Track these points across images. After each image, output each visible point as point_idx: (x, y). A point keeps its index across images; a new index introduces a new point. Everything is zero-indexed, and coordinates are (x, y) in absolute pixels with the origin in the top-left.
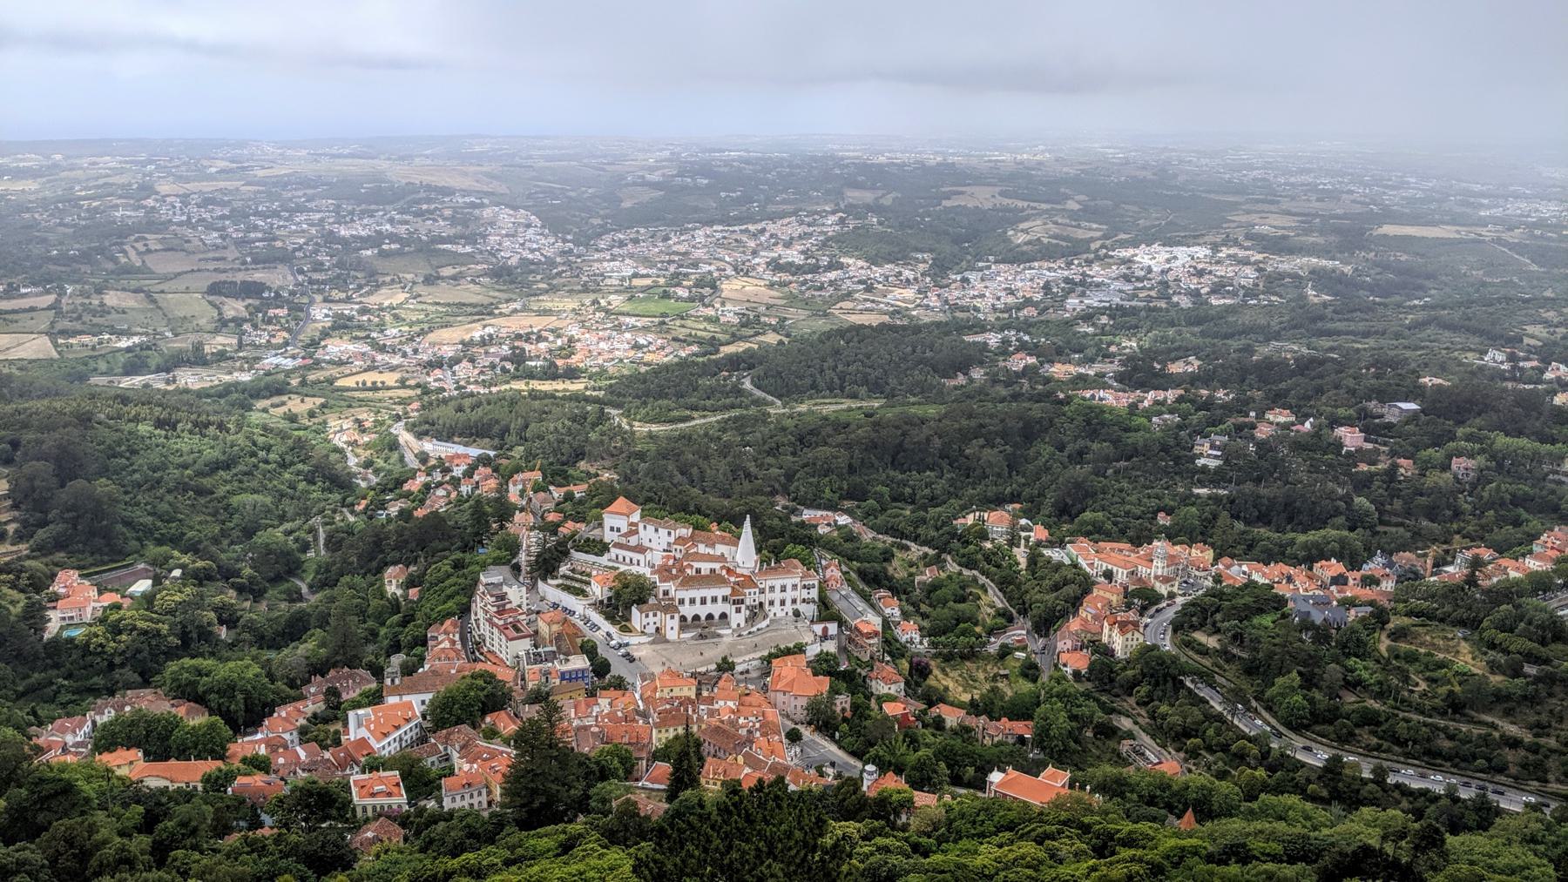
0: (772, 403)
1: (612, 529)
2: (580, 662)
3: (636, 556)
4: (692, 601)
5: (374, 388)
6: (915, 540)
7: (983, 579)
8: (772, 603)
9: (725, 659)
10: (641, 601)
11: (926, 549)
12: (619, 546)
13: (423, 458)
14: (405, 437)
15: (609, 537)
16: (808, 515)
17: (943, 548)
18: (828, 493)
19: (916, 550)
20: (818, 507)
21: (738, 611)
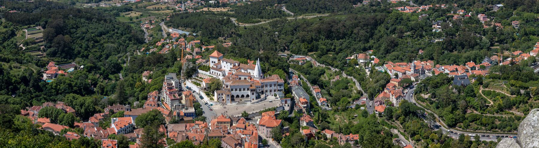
0: (289, 15)
1: (212, 62)
2: (192, 110)
3: (219, 73)
4: (236, 90)
5: (158, 10)
6: (332, 66)
7: (354, 80)
8: (266, 91)
9: (245, 112)
10: (218, 89)
11: (336, 69)
12: (213, 68)
13: (169, 34)
14: (163, 26)
15: (211, 65)
16: (296, 57)
17: (342, 69)
18: (303, 50)
19: (333, 69)
20: (300, 54)
21: (253, 94)
